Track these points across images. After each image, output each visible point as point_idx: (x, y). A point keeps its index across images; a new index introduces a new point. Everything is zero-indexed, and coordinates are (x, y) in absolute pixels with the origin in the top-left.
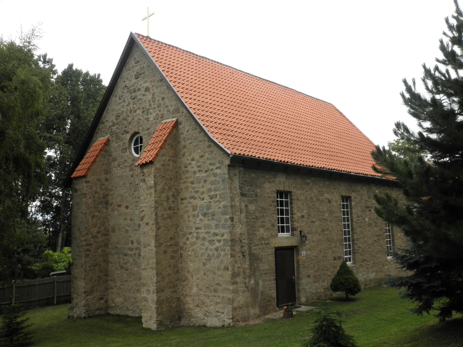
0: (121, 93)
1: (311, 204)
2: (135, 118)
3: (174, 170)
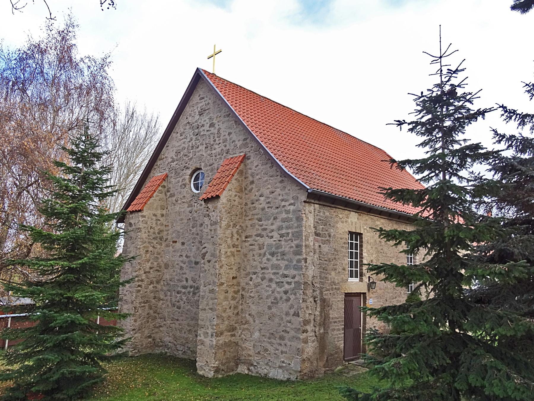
0: (182, 130)
1: (379, 248)
2: (197, 154)
3: (239, 206)
